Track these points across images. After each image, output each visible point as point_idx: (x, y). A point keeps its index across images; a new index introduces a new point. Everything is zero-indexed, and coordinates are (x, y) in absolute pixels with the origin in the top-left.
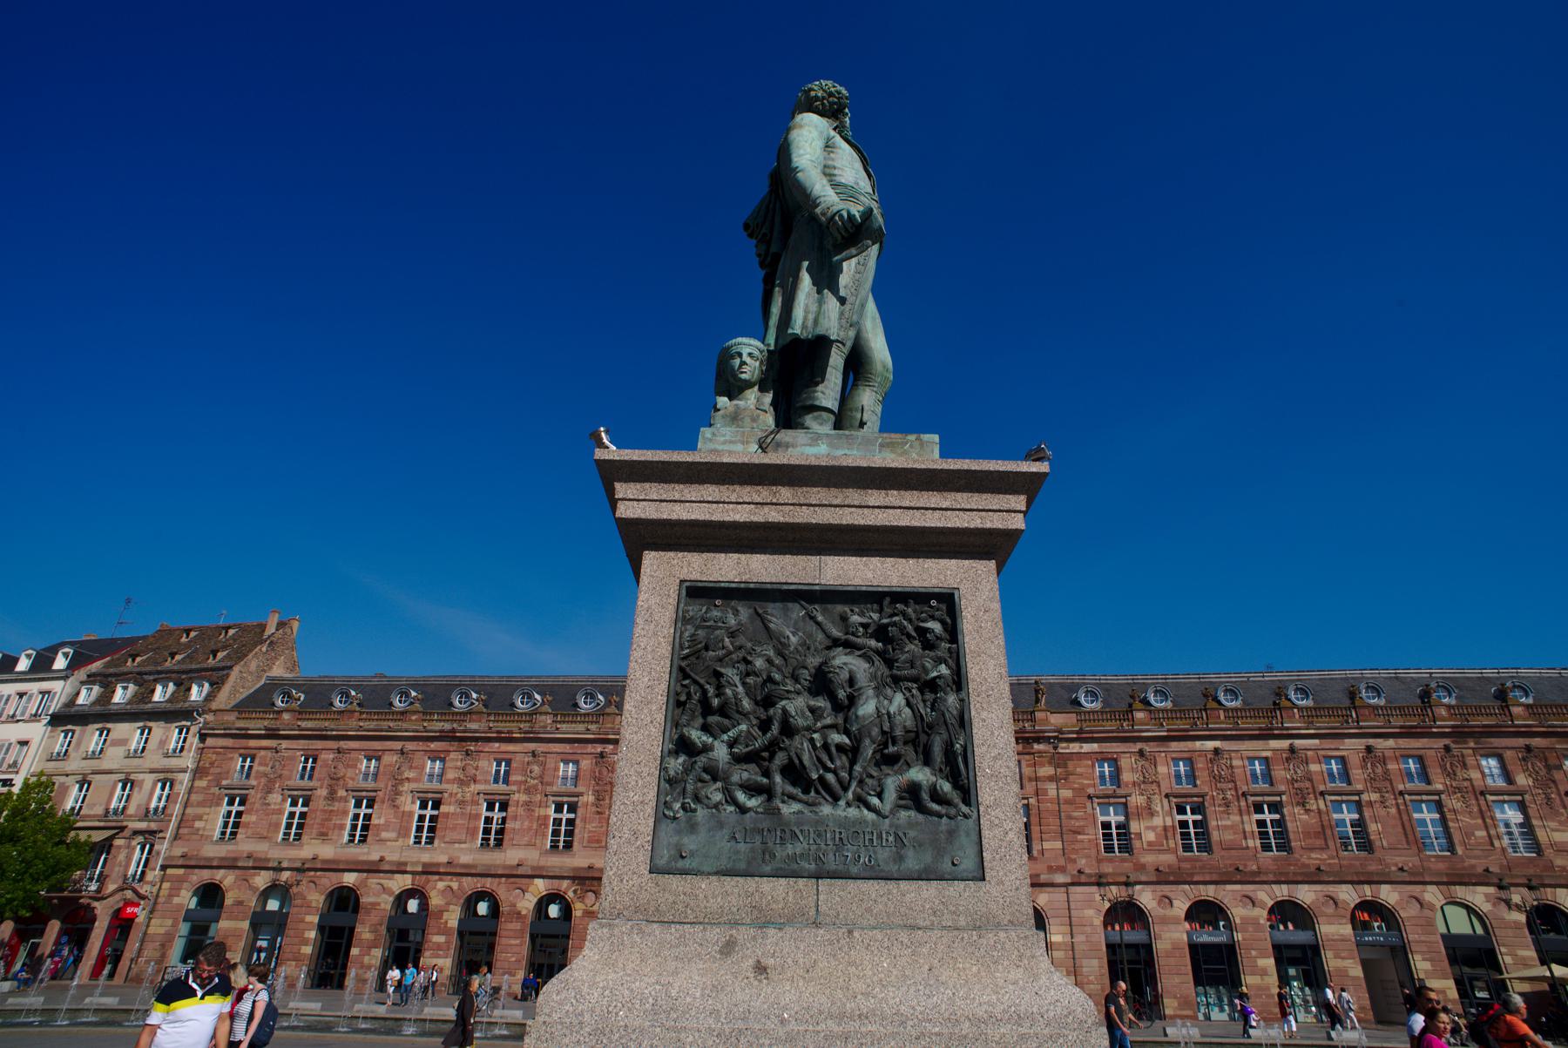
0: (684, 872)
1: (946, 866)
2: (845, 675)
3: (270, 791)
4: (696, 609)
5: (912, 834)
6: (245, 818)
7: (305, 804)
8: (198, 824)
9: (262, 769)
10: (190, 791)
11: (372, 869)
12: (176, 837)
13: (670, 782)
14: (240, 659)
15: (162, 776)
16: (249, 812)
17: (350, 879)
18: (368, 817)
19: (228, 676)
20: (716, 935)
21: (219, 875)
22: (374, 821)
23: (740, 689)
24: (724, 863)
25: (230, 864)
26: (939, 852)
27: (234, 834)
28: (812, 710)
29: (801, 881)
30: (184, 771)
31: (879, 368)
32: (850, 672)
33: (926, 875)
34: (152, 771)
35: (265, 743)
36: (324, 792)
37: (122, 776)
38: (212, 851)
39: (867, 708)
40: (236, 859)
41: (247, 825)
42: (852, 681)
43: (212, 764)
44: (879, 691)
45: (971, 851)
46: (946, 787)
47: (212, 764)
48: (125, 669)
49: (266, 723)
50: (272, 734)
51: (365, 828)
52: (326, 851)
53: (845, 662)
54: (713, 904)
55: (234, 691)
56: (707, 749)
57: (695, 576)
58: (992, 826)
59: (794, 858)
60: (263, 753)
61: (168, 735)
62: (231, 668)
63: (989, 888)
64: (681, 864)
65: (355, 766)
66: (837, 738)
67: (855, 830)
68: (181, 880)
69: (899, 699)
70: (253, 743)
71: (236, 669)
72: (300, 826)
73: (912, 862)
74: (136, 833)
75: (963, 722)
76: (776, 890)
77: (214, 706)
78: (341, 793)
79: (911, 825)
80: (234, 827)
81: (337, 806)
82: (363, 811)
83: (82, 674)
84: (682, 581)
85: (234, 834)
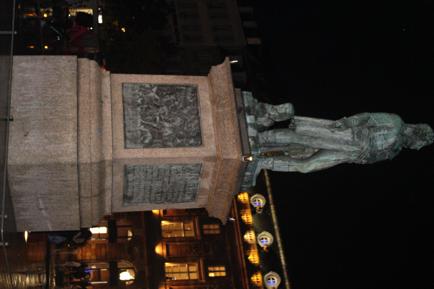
0: (123, 89)
1: (128, 142)
4: (190, 89)
5: (135, 134)
23: (169, 99)
24: (125, 96)
26: (131, 140)
28: (164, 113)
29: (122, 112)
33: (125, 138)
39: (166, 125)
44: (171, 128)
45: (132, 146)
46: (147, 141)
54: (116, 95)
56: (152, 92)
57: (199, 88)
58: (138, 151)
59: (127, 110)
64: (124, 89)
67: (135, 122)
69: (170, 132)
73: (128, 134)
75: (164, 146)
76: (120, 106)
79: (137, 134)
84: (197, 85)
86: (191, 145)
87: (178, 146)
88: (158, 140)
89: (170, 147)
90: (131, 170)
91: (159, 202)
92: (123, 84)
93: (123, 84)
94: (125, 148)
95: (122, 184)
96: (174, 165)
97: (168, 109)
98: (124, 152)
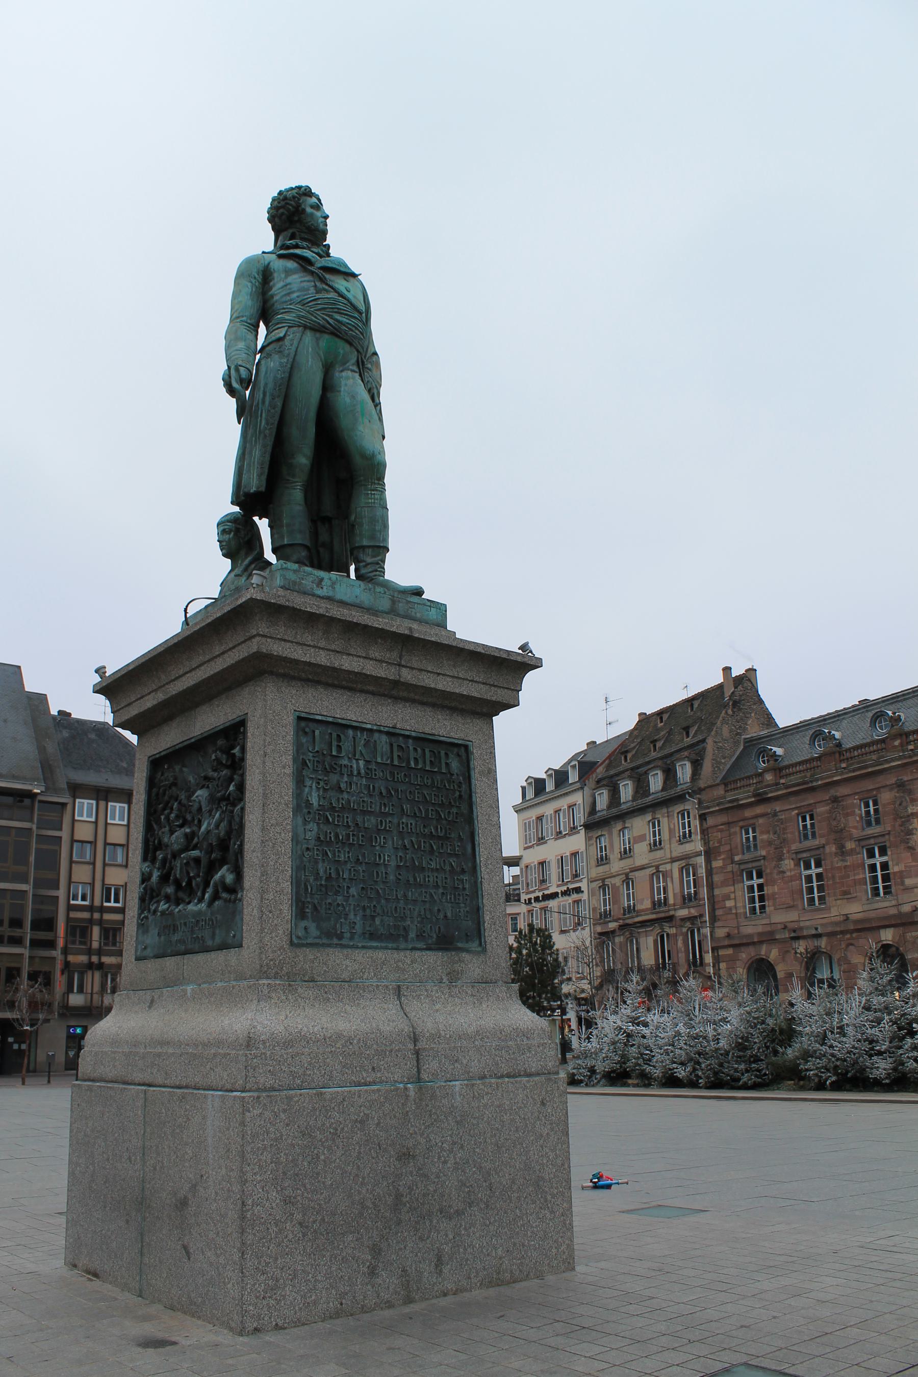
2: (196, 806)
3: (780, 858)
6: (767, 891)
7: (818, 865)
8: (729, 904)
9: (765, 837)
10: (710, 872)
11: (903, 922)
12: (714, 918)
13: (142, 899)
14: (710, 730)
15: (683, 863)
16: (772, 882)
17: (887, 936)
18: (885, 866)
19: (704, 749)
20: (148, 995)
21: (763, 950)
22: (894, 869)
23: (167, 828)
25: (768, 938)
27: (763, 908)
28: (186, 835)
30: (698, 854)
31: (358, 460)
32: (200, 802)
34: (673, 860)
35: (759, 810)
36: (832, 848)
37: (653, 870)
38: (751, 928)
40: (772, 933)
41: (773, 896)
42: (200, 809)
43: (720, 842)
46: (230, 878)
47: (720, 842)
48: (621, 768)
49: (752, 789)
50: (762, 799)
51: (886, 878)
52: (855, 909)
53: (201, 794)
55: (717, 764)
60: (761, 821)
61: (669, 823)
62: (703, 741)
63: (245, 952)
64: (146, 953)
65: (853, 814)
66: (195, 853)
68: (732, 960)
70: (748, 813)
71: (710, 741)
72: (821, 888)
74: (683, 920)
75: (241, 826)
76: (170, 963)
77: (702, 784)
78: (849, 845)
80: (760, 900)
81: (849, 861)
82: (878, 860)
83: (591, 783)
85: (763, 908)
86: (243, 750)
87: (241, 788)
88: (227, 850)
89: (243, 809)
90: (318, 927)
92: (137, 959)
93: (137, 959)
94: (241, 946)
95: (380, 955)
96: (298, 795)
97: (181, 826)
98: (248, 947)
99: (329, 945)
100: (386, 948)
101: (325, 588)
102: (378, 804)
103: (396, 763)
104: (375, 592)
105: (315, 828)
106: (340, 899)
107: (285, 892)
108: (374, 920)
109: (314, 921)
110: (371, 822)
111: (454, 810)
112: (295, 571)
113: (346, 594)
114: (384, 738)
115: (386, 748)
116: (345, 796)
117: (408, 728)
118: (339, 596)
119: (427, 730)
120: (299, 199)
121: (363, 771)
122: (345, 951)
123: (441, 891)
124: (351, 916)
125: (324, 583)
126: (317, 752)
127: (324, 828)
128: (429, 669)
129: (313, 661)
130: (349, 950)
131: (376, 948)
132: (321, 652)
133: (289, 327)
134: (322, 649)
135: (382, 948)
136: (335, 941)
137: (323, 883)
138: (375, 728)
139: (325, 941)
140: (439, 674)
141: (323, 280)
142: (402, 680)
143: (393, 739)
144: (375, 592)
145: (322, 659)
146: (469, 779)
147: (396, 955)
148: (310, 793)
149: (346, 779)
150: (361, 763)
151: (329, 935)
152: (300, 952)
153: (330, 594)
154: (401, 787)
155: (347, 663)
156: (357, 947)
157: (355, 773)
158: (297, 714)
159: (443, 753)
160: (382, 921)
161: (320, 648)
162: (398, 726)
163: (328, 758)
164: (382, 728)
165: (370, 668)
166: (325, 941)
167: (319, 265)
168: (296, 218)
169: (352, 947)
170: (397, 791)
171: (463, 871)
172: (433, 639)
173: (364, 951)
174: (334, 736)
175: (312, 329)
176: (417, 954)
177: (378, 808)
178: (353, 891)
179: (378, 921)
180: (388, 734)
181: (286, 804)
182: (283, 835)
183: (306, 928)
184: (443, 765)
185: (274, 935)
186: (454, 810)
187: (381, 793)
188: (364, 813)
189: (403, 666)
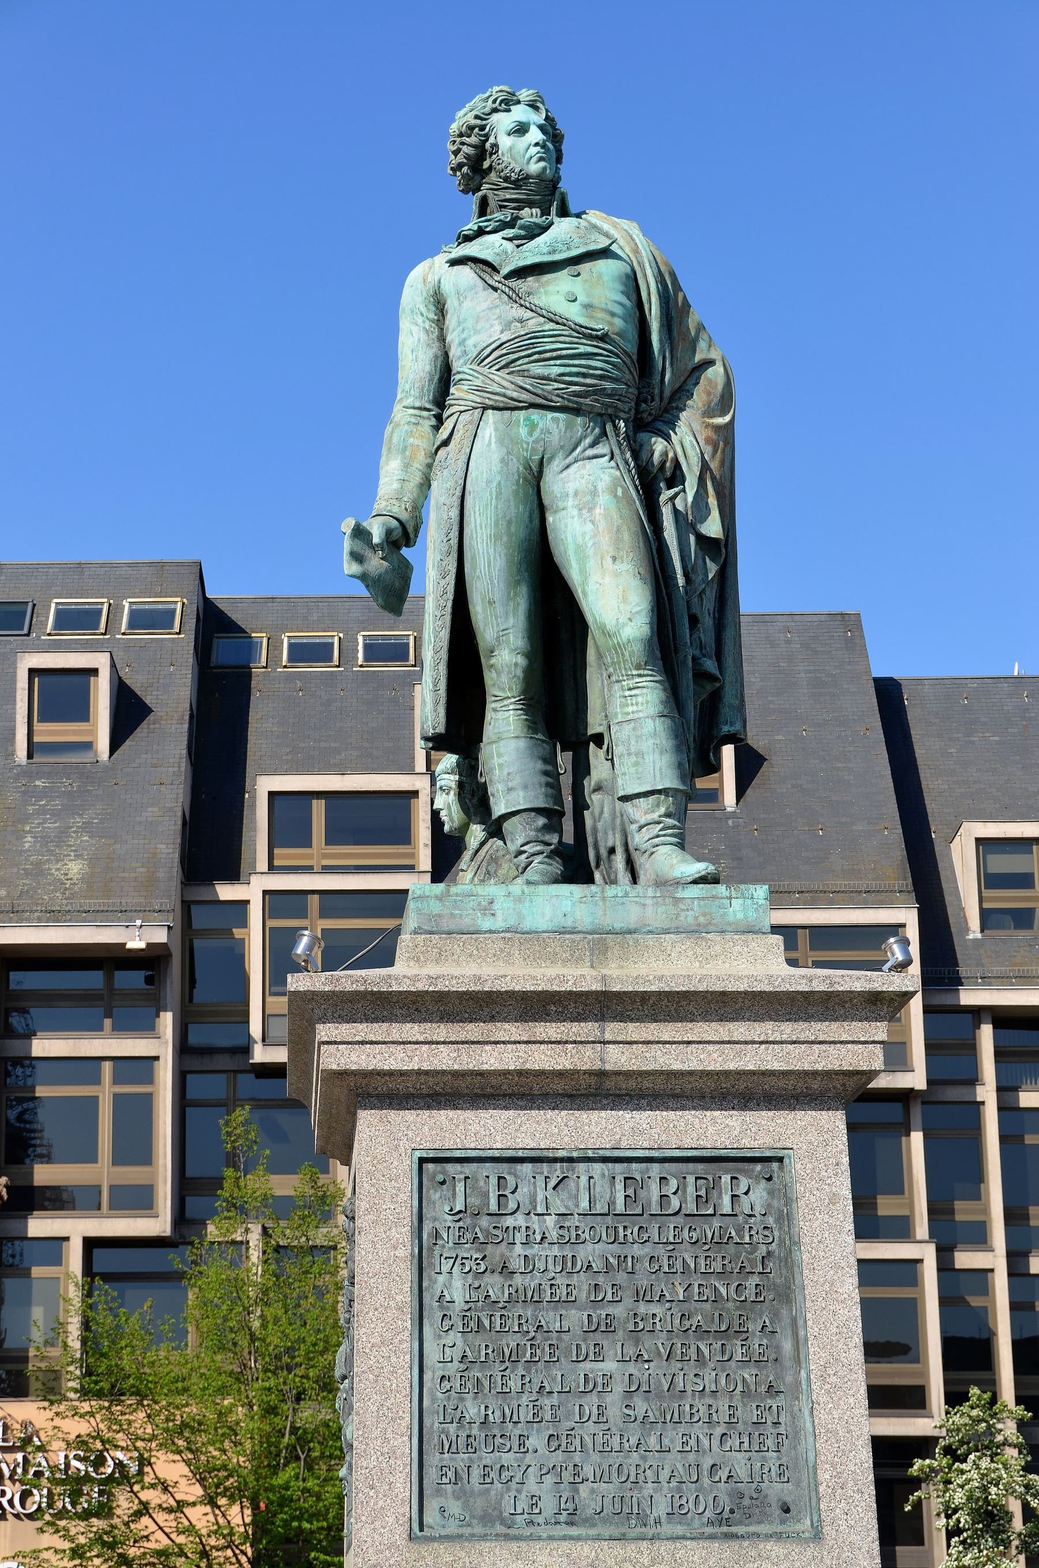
91: (787, 1346)
99: (484, 1537)
100: (598, 1538)
101: (499, 913)
102: (585, 1287)
103: (620, 1207)
104: (604, 899)
105: (460, 1342)
106: (507, 1458)
107: (399, 1453)
108: (577, 1491)
109: (459, 1499)
110: (576, 1318)
111: (753, 1281)
112: (440, 898)
113: (543, 915)
114: (597, 1168)
115: (601, 1187)
116: (518, 1280)
117: (646, 1145)
118: (527, 925)
119: (688, 1142)
120: (482, 128)
121: (553, 1235)
122: (514, 1546)
123: (718, 1431)
124: (532, 1486)
125: (496, 906)
126: (460, 1212)
127: (480, 1341)
128: (666, 1038)
129: (426, 1067)
130: (523, 1544)
131: (578, 1539)
132: (441, 1047)
133: (461, 412)
134: (444, 1043)
135: (587, 1538)
136: (499, 1529)
137: (475, 1431)
138: (575, 1154)
139: (478, 1530)
140: (689, 1043)
141: (515, 298)
142: (608, 1067)
143: (619, 1167)
144: (604, 899)
145: (445, 1059)
146: (786, 1218)
147: (618, 1549)
148: (448, 1286)
149: (518, 1249)
150: (550, 1221)
151: (485, 1519)
152: (424, 1549)
153: (512, 922)
154: (637, 1250)
155: (490, 1059)
156: (540, 1538)
157: (538, 1238)
158: (418, 1154)
159: (726, 1179)
160: (593, 1491)
161: (438, 1043)
162: (623, 1145)
163: (485, 1222)
164: (590, 1154)
165: (542, 1059)
166: (478, 1530)
167: (505, 271)
168: (486, 165)
169: (531, 1538)
170: (622, 1259)
171: (772, 1390)
172: (654, 988)
173: (555, 1544)
174: (493, 1181)
175: (494, 408)
176: (664, 1548)
177: (584, 1295)
178: (531, 1443)
179: (584, 1490)
180: (605, 1160)
181: (399, 1308)
182: (394, 1359)
183: (442, 1510)
184: (726, 1199)
185: (377, 1524)
186: (753, 1281)
187: (589, 1267)
188: (556, 1303)
189: (609, 1042)
